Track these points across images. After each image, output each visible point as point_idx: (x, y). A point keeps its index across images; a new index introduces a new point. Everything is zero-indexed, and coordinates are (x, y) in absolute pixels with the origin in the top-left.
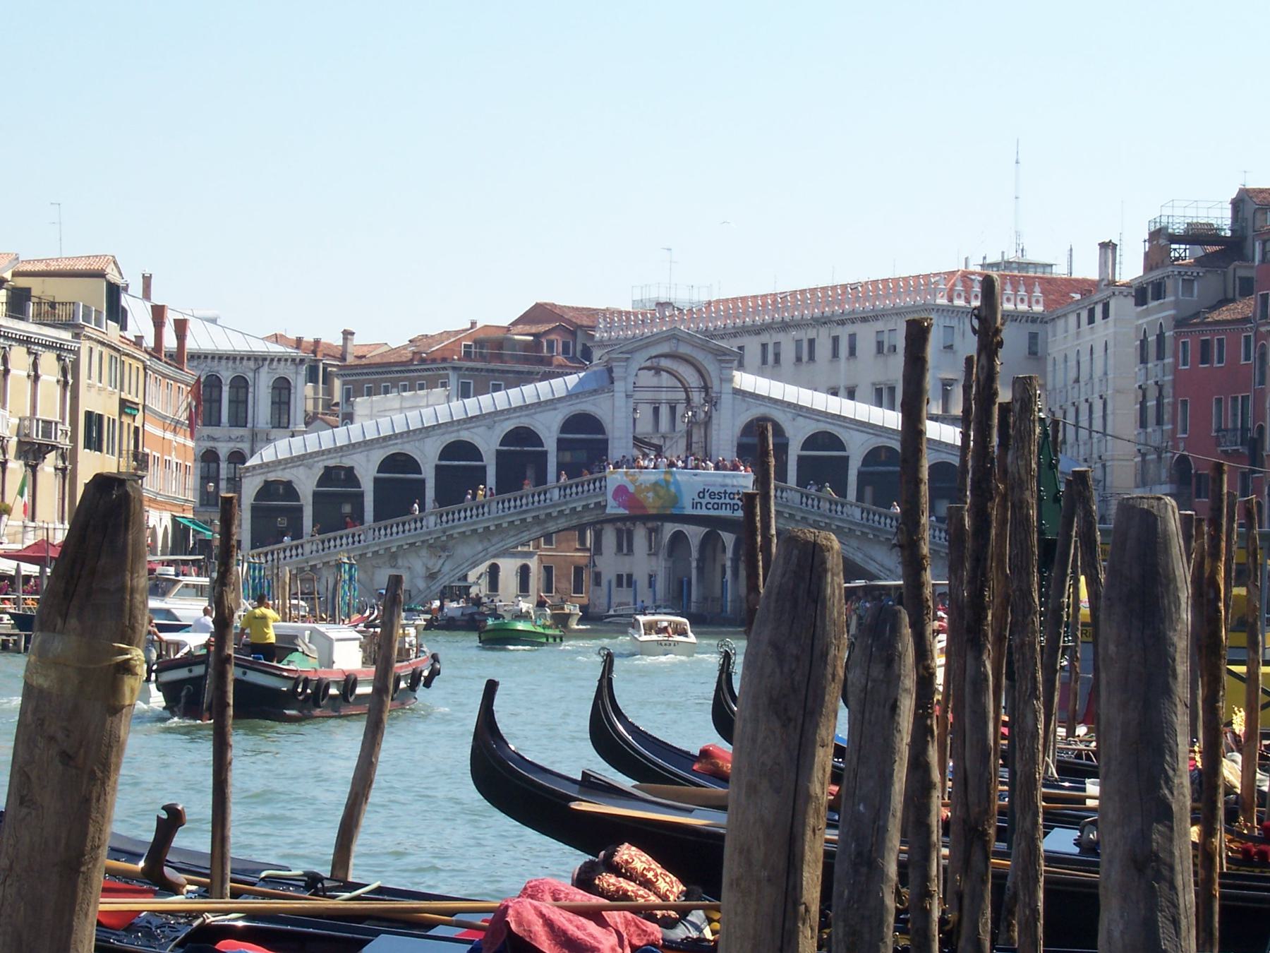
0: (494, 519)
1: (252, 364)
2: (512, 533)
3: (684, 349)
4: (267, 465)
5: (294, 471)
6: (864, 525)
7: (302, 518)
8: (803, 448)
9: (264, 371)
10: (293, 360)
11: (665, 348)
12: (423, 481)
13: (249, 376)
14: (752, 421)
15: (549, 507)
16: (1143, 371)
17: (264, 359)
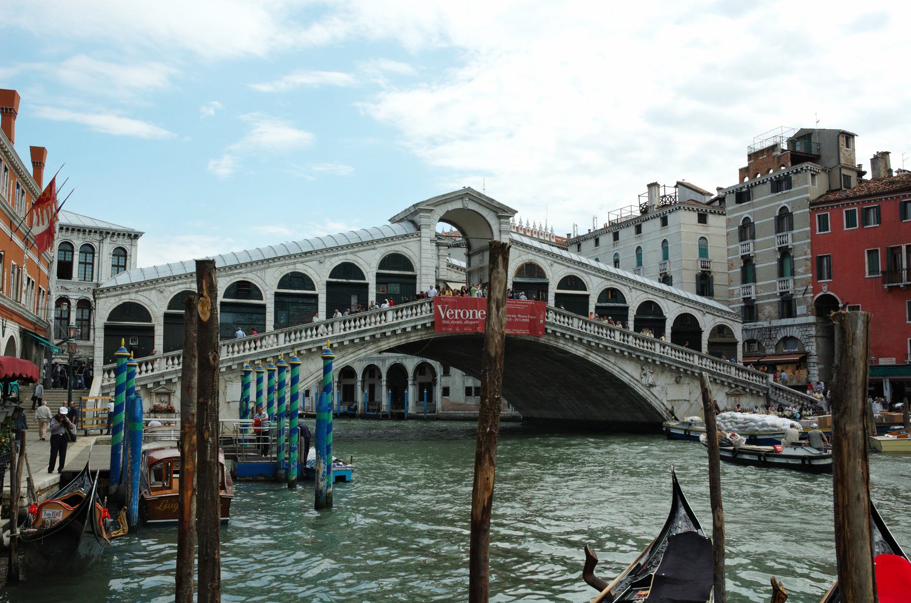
0: (337, 337)
1: (98, 237)
2: (350, 350)
3: (472, 206)
4: (121, 287)
5: (146, 294)
6: (623, 345)
7: (153, 337)
8: (558, 288)
9: (108, 240)
10: (129, 235)
11: (458, 205)
12: (263, 307)
13: (96, 245)
14: (522, 266)
15: (385, 327)
16: (751, 244)
17: (108, 233)
